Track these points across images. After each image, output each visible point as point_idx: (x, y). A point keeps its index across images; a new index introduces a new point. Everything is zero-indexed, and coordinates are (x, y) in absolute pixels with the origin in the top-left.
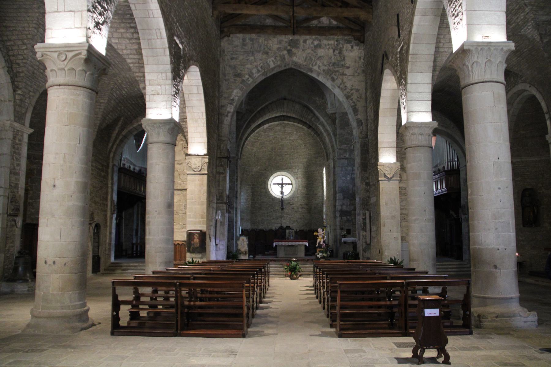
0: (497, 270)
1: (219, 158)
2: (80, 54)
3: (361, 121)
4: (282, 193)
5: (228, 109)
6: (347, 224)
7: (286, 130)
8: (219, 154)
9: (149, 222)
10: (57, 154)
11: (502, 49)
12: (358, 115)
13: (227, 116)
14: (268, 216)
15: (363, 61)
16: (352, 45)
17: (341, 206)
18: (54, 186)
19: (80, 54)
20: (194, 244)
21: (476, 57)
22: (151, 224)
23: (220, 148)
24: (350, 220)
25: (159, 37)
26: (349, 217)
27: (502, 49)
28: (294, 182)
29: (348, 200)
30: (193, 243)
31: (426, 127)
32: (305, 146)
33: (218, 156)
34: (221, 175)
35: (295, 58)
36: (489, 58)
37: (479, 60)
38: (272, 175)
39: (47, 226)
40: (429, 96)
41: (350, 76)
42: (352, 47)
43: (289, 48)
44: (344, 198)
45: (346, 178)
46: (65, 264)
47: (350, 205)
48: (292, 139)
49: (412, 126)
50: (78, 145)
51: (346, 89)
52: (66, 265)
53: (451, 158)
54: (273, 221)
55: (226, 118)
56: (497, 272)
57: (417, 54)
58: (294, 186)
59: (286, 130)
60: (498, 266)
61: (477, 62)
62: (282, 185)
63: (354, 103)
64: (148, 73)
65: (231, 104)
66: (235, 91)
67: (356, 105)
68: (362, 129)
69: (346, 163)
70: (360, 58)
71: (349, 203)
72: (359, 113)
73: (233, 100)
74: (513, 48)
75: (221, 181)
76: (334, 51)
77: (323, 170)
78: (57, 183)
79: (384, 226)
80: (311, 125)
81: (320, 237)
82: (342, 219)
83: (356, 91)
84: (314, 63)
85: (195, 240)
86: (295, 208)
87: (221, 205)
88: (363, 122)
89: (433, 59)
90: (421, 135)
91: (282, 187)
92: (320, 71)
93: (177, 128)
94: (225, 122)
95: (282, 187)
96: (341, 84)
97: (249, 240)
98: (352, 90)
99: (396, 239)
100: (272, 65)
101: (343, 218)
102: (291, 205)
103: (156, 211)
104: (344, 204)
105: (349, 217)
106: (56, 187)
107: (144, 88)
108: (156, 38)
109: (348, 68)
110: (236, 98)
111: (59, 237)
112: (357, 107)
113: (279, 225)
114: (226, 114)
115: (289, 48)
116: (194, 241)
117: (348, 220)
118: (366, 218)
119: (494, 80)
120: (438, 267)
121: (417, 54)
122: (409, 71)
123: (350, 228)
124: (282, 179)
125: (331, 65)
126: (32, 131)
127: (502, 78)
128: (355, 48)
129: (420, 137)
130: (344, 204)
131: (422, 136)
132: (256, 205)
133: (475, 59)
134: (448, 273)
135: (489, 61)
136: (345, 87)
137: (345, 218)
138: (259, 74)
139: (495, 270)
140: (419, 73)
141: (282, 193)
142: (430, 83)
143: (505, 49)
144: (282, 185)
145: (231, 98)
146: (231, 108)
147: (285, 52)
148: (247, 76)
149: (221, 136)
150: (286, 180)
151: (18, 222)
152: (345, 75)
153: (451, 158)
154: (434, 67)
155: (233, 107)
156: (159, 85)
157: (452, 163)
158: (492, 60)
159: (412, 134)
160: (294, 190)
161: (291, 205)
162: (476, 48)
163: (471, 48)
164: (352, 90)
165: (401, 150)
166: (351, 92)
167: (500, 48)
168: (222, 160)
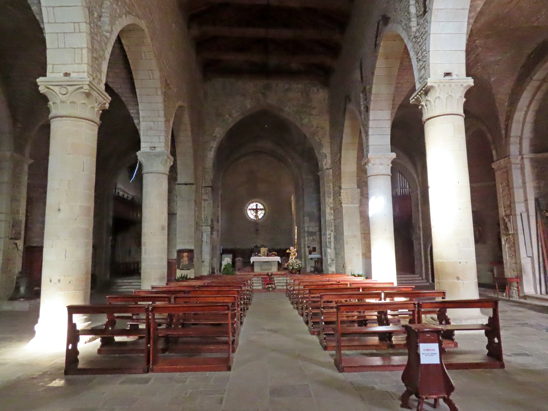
0: (460, 281)
1: (204, 187)
2: (82, 88)
3: (326, 154)
4: (256, 216)
5: (212, 145)
8: (204, 183)
9: (145, 243)
10: (61, 180)
11: (462, 85)
15: (327, 102)
16: (317, 88)
17: (308, 227)
18: (59, 210)
19: (82, 88)
20: (183, 262)
21: (438, 92)
22: (147, 244)
23: (205, 178)
25: (151, 78)
27: (462, 85)
28: (266, 208)
30: (182, 260)
31: (386, 158)
33: (204, 185)
34: (206, 202)
35: (269, 100)
36: (450, 93)
37: (441, 96)
39: (52, 247)
40: (389, 131)
41: (316, 115)
42: (318, 90)
43: (263, 91)
46: (70, 282)
47: (315, 227)
49: (373, 157)
50: (81, 172)
51: (312, 127)
52: (71, 282)
53: (404, 185)
56: (460, 283)
57: (379, 94)
58: (267, 211)
60: (460, 278)
61: (439, 97)
62: (256, 210)
63: (320, 139)
64: (141, 110)
65: (214, 140)
66: (217, 129)
67: (321, 141)
68: (327, 161)
70: (324, 100)
71: (314, 226)
73: (215, 137)
74: (472, 84)
75: (206, 207)
76: (302, 94)
78: (62, 207)
79: (347, 244)
81: (292, 254)
82: (308, 239)
83: (321, 129)
84: (285, 105)
85: (184, 258)
87: (206, 227)
88: (327, 155)
89: (392, 99)
90: (381, 165)
91: (256, 212)
92: (290, 111)
93: (169, 160)
95: (256, 212)
96: (308, 123)
98: (317, 127)
99: (358, 255)
100: (249, 106)
103: (151, 233)
106: (61, 211)
107: (139, 124)
108: (148, 78)
109: (314, 108)
110: (218, 135)
111: (64, 257)
113: (255, 245)
115: (263, 91)
116: (183, 259)
117: (313, 240)
118: (330, 238)
119: (454, 113)
120: (400, 279)
121: (379, 94)
122: (371, 109)
123: (315, 246)
124: (257, 205)
125: (300, 106)
126: (31, 161)
127: (461, 112)
128: (321, 90)
129: (380, 167)
131: (383, 165)
133: (438, 95)
134: (415, 284)
135: (451, 96)
136: (312, 125)
137: (311, 238)
138: (237, 115)
139: (458, 281)
140: (380, 111)
141: (256, 216)
142: (389, 120)
143: (465, 85)
144: (256, 210)
145: (214, 135)
147: (260, 95)
148: (227, 116)
149: (205, 168)
150: (260, 206)
151: (19, 245)
152: (312, 115)
153: (404, 185)
154: (393, 105)
155: (215, 143)
156: (153, 121)
157: (404, 190)
158: (453, 95)
159: (373, 164)
162: (439, 85)
163: (434, 85)
164: (317, 127)
165: (361, 179)
166: (317, 130)
167: (460, 84)
168: (207, 188)
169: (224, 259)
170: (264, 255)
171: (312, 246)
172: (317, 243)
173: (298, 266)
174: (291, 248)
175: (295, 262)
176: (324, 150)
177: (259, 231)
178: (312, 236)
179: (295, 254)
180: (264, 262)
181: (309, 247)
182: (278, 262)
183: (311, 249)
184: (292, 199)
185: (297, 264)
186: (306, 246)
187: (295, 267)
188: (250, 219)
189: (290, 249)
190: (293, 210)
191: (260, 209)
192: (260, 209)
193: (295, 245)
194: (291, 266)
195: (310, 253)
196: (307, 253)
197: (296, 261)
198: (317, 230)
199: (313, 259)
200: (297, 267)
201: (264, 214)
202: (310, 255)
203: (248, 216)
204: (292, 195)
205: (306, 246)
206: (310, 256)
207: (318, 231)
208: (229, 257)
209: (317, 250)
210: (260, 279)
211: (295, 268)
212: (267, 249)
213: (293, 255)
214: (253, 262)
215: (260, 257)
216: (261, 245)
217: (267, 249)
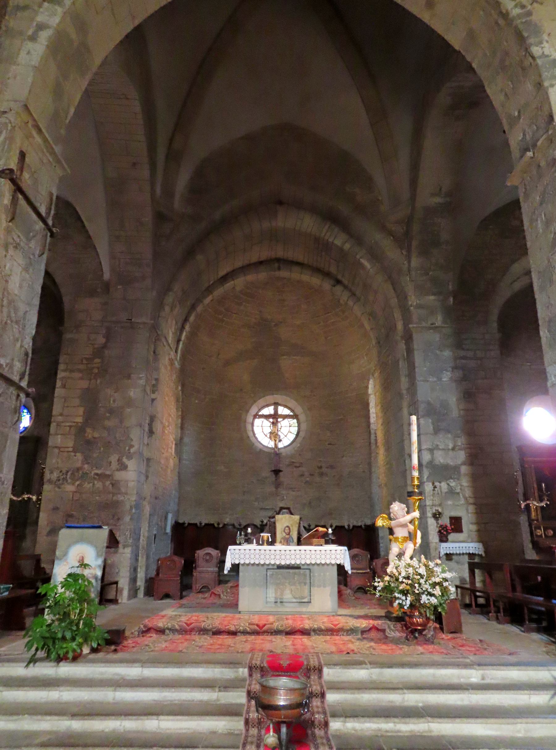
6: (450, 502)
7: (284, 300)
12: (541, 43)
13: (33, 38)
14: (244, 493)
17: (431, 451)
24: (458, 490)
26: (453, 484)
28: (299, 410)
29: (449, 436)
32: (326, 338)
38: (255, 402)
44: (437, 431)
45: (440, 379)
47: (453, 449)
48: (298, 322)
54: (256, 503)
55: (30, 45)
58: (302, 417)
59: (284, 300)
63: (523, 7)
67: (529, 14)
69: (438, 339)
71: (450, 447)
72: (545, 37)
77: (367, 387)
80: (340, 277)
81: (400, 533)
82: (435, 487)
86: (306, 474)
91: (274, 424)
94: (23, 57)
95: (274, 424)
97: (197, 550)
101: (437, 484)
102: (296, 467)
104: (437, 447)
105: (453, 484)
112: (534, 18)
114: (30, 32)
117: (451, 492)
130: (437, 447)
132: (218, 468)
137: (444, 485)
146: (54, 14)
155: (59, 10)
160: (304, 426)
161: (296, 467)
169: (65, 554)
170: (287, 541)
171: (448, 513)
172: (462, 501)
173: (437, 591)
174: (397, 507)
175: (422, 571)
176: (545, 44)
177: (281, 474)
178: (447, 478)
179: (411, 537)
180: (280, 567)
181: (437, 516)
182: (340, 568)
183: (445, 521)
184: (370, 391)
185: (434, 585)
186: (429, 515)
187: (424, 599)
188: (260, 446)
189: (389, 514)
190: (373, 419)
191: (285, 417)
192: (285, 417)
193: (410, 494)
194: (405, 593)
195: (443, 538)
196: (434, 537)
197: (426, 566)
198: (459, 462)
199: (454, 557)
200: (434, 601)
201: (297, 435)
202: (444, 545)
203: (256, 438)
204: (369, 380)
205: (429, 515)
206: (446, 548)
207: (464, 464)
208: (90, 542)
209: (464, 528)
210: (243, 672)
211: (424, 606)
212: (297, 518)
213: (405, 539)
214: (236, 568)
215: (266, 547)
216: (282, 508)
217: (297, 518)
